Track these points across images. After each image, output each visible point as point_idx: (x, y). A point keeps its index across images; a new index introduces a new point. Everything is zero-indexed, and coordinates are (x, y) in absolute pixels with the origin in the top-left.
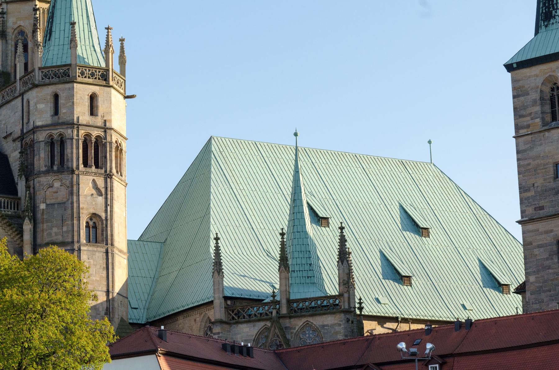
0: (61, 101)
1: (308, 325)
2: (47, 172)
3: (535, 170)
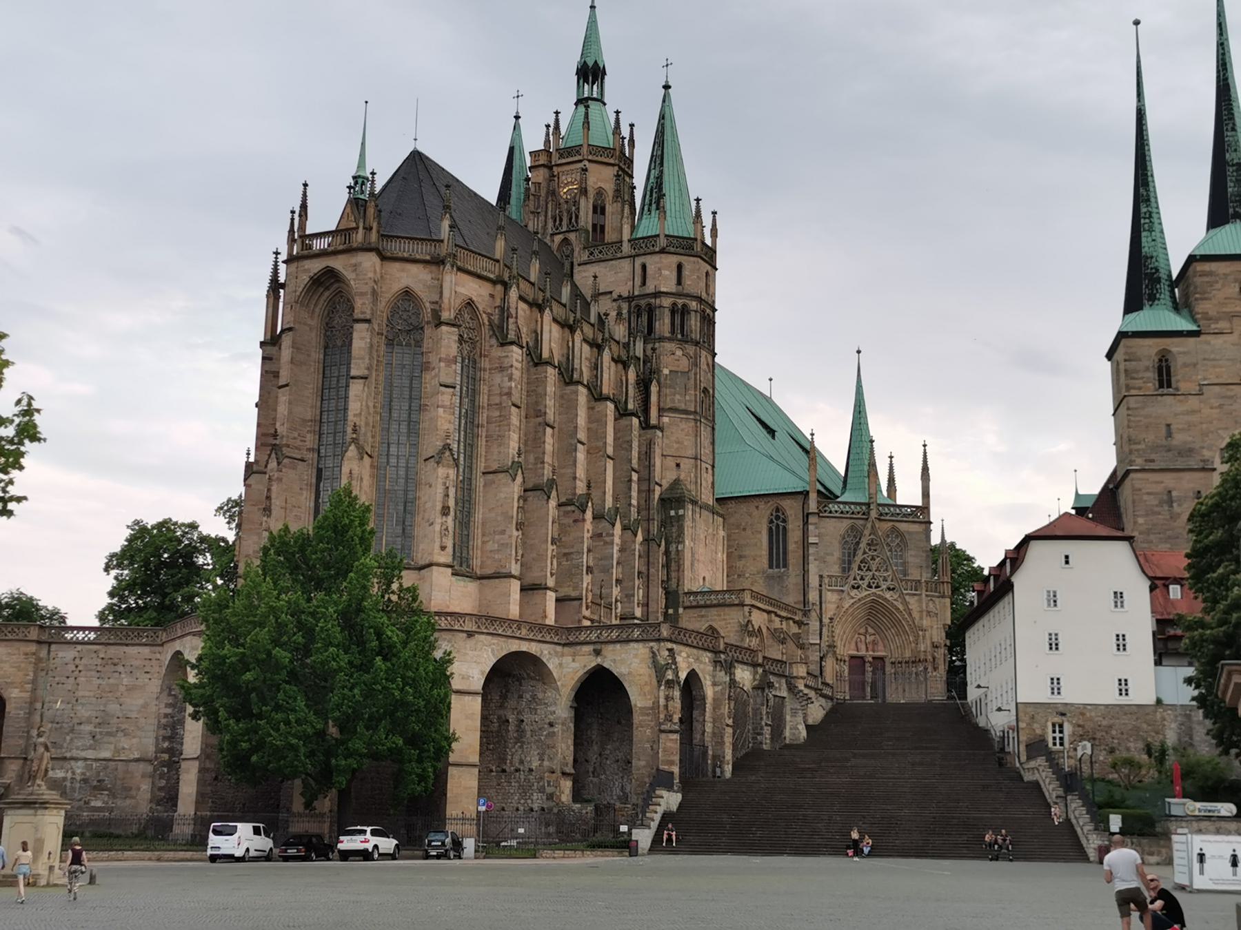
0: (686, 272)
1: (894, 529)
2: (670, 340)
3: (1147, 427)
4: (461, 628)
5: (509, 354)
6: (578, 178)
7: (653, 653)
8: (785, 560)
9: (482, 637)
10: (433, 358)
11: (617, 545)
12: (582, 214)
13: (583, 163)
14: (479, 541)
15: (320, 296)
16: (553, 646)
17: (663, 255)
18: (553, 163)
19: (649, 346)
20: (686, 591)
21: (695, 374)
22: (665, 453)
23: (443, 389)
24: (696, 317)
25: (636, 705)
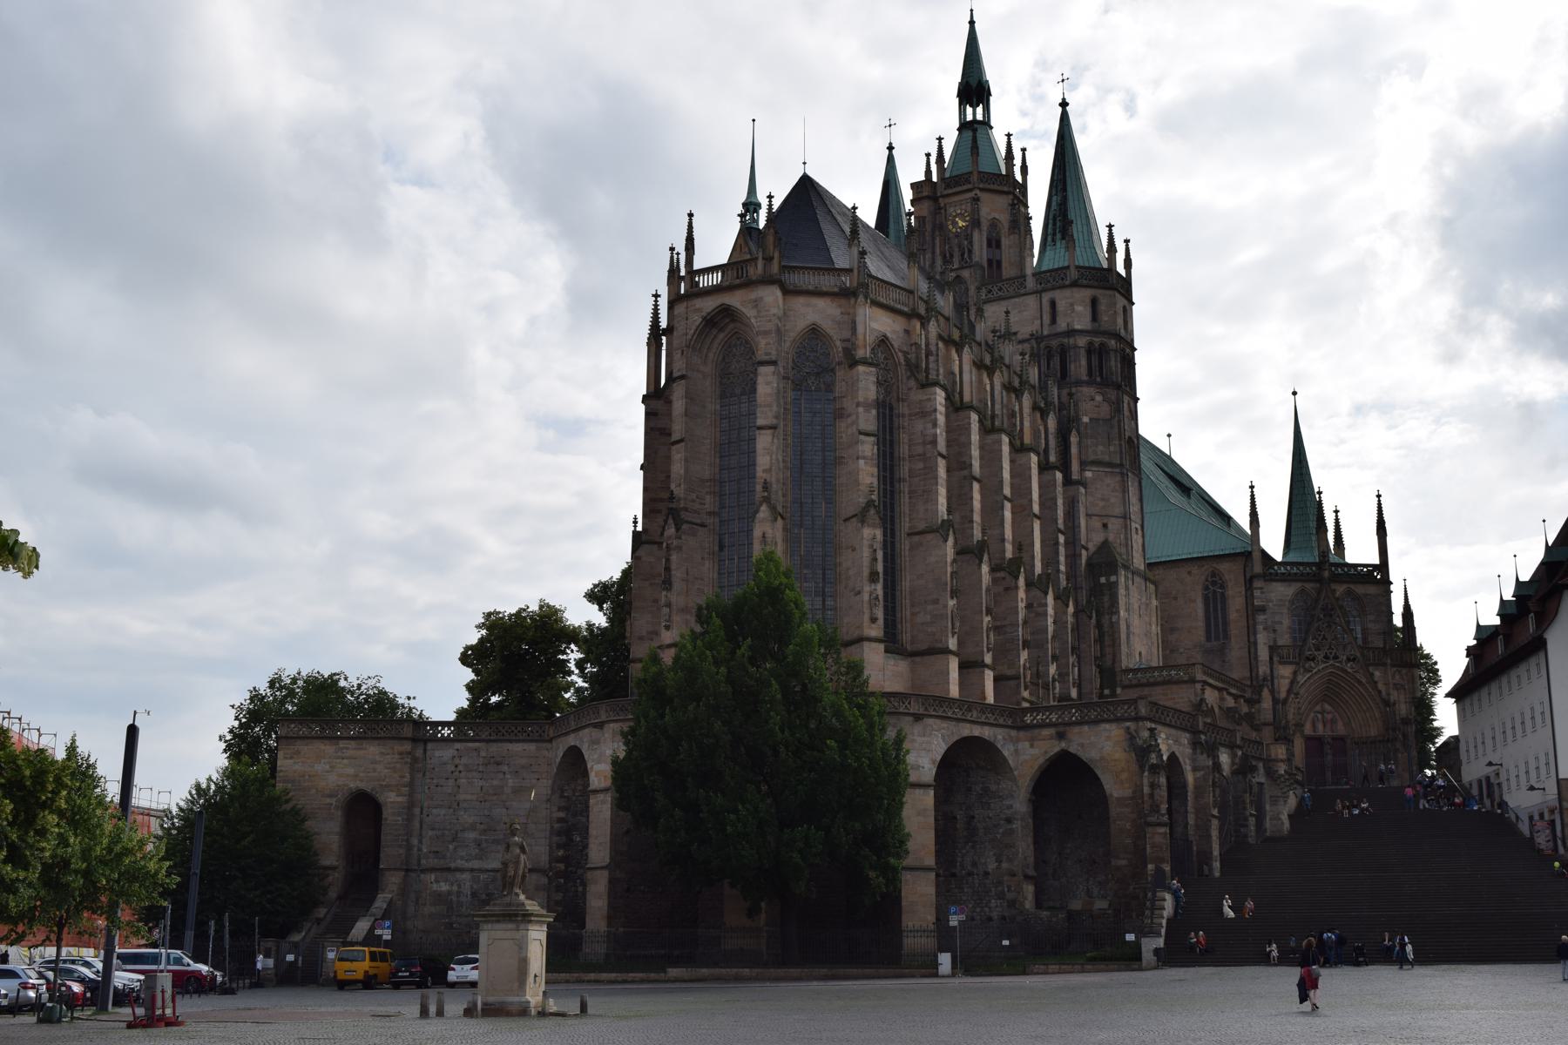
0: (1102, 307)
1: (1349, 593)
2: (1088, 383)
4: (906, 711)
5: (933, 397)
6: (969, 209)
7: (1129, 733)
8: (1225, 631)
9: (931, 721)
10: (848, 404)
11: (1051, 616)
12: (976, 247)
13: (974, 193)
14: (908, 613)
15: (713, 339)
16: (1006, 730)
17: (1075, 289)
18: (939, 194)
19: (1065, 392)
20: (1124, 668)
21: (1119, 421)
22: (1090, 512)
23: (862, 437)
24: (1116, 357)
25: (1111, 795)
